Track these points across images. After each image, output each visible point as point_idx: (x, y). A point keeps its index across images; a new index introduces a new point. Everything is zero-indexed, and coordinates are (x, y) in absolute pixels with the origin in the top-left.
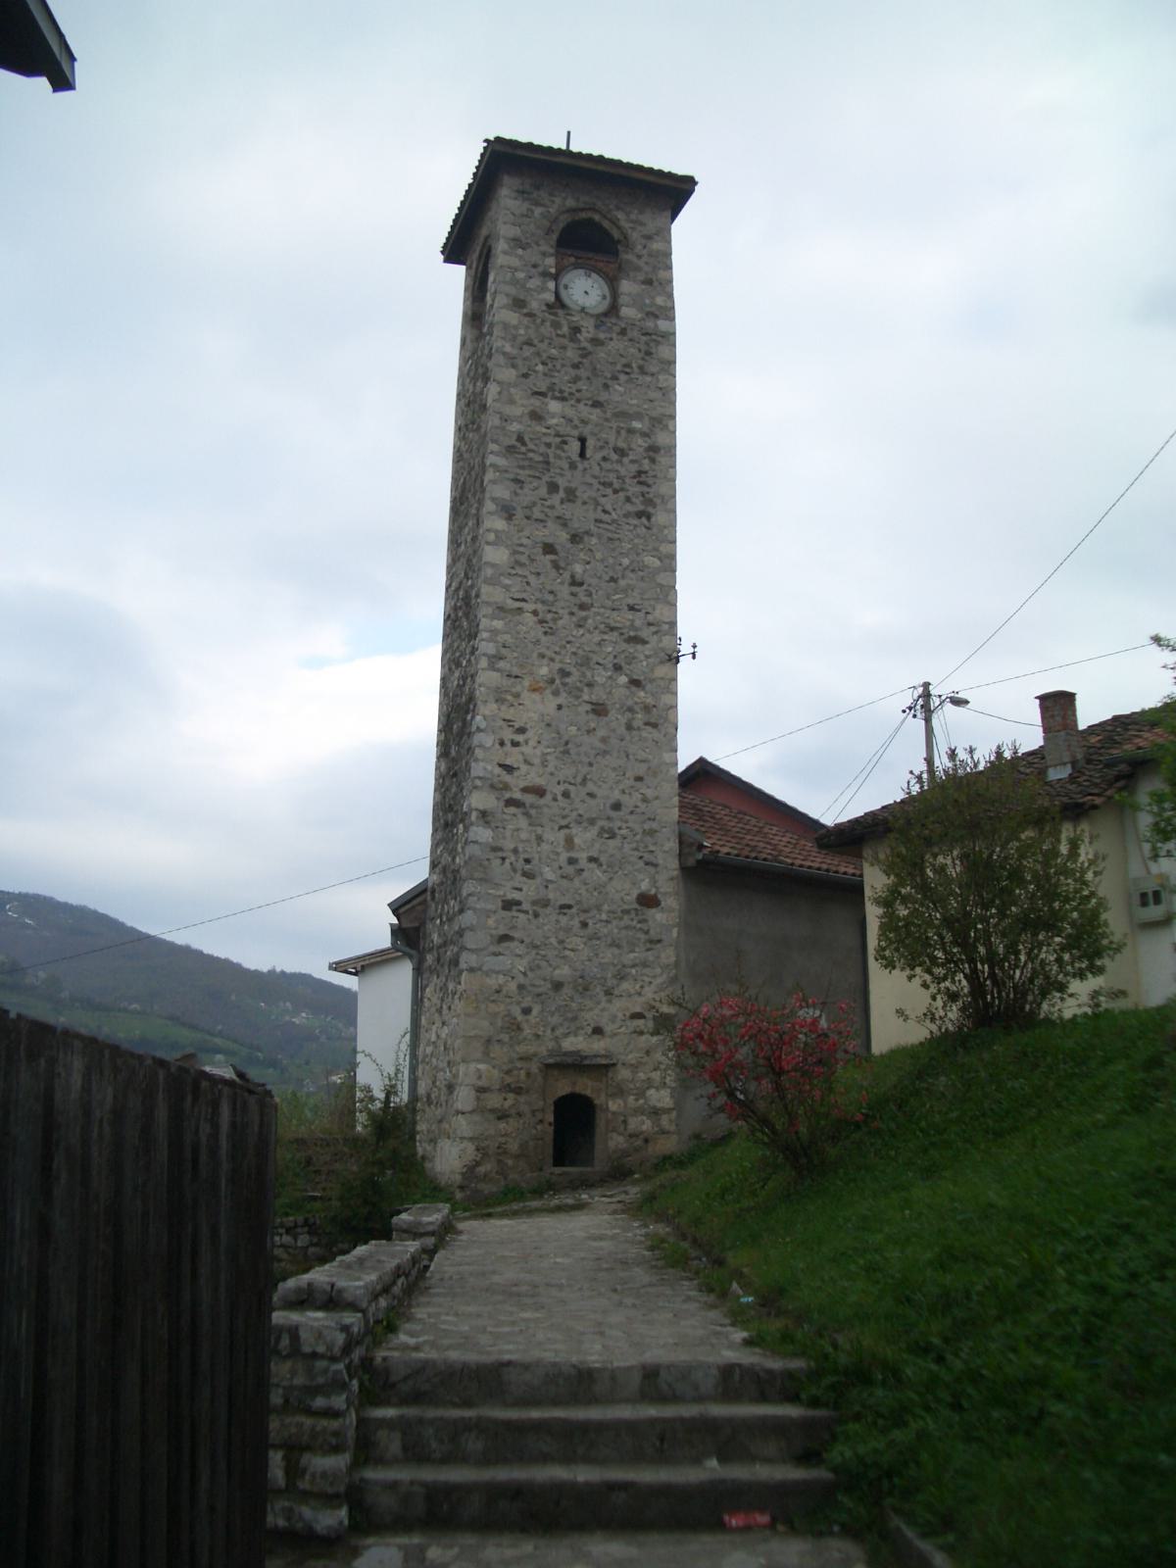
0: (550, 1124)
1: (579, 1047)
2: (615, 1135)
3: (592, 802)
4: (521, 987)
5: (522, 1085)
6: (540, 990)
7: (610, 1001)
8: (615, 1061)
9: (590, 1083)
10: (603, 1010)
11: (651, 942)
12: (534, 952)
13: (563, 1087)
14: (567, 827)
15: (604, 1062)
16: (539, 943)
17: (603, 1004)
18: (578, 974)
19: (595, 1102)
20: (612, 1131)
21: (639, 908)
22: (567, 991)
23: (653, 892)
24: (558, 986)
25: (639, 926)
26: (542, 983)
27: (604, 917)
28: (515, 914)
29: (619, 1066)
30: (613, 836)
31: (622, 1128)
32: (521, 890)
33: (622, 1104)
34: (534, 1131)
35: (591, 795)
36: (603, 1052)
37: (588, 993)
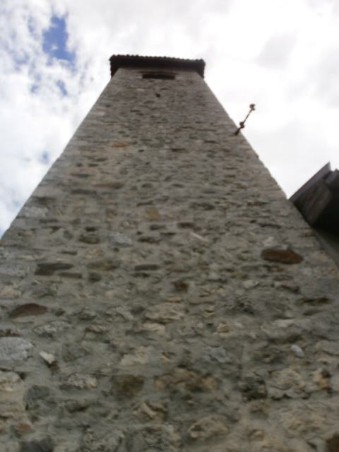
3: (179, 190)
4: (37, 394)
6: (82, 399)
7: (258, 413)
10: (251, 435)
11: (310, 301)
12: (81, 328)
14: (150, 203)
16: (93, 314)
17: (246, 422)
18: (174, 360)
21: (270, 264)
22: (151, 396)
23: (285, 247)
24: (128, 387)
25: (277, 284)
26: (92, 382)
27: (214, 276)
28: (58, 279)
30: (210, 208)
32: (74, 253)
35: (177, 186)
37: (204, 397)
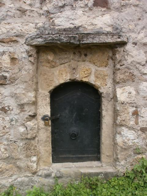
0: (44, 118)
1: (77, 23)
2: (125, 131)
5: (6, 74)
8: (125, 40)
9: (93, 68)
13: (61, 75)
15: (110, 40)
19: (101, 90)
20: (122, 125)
29: (129, 47)
31: (132, 123)
33: (134, 93)
34: (22, 129)
36: (109, 29)
